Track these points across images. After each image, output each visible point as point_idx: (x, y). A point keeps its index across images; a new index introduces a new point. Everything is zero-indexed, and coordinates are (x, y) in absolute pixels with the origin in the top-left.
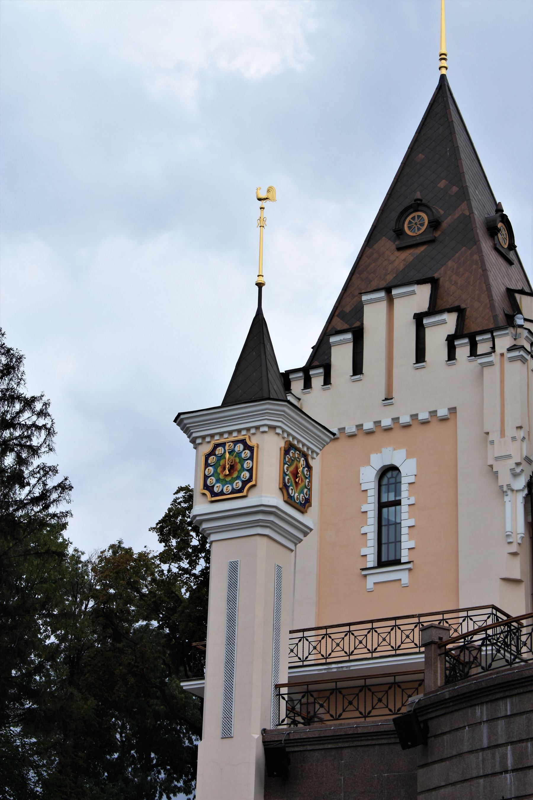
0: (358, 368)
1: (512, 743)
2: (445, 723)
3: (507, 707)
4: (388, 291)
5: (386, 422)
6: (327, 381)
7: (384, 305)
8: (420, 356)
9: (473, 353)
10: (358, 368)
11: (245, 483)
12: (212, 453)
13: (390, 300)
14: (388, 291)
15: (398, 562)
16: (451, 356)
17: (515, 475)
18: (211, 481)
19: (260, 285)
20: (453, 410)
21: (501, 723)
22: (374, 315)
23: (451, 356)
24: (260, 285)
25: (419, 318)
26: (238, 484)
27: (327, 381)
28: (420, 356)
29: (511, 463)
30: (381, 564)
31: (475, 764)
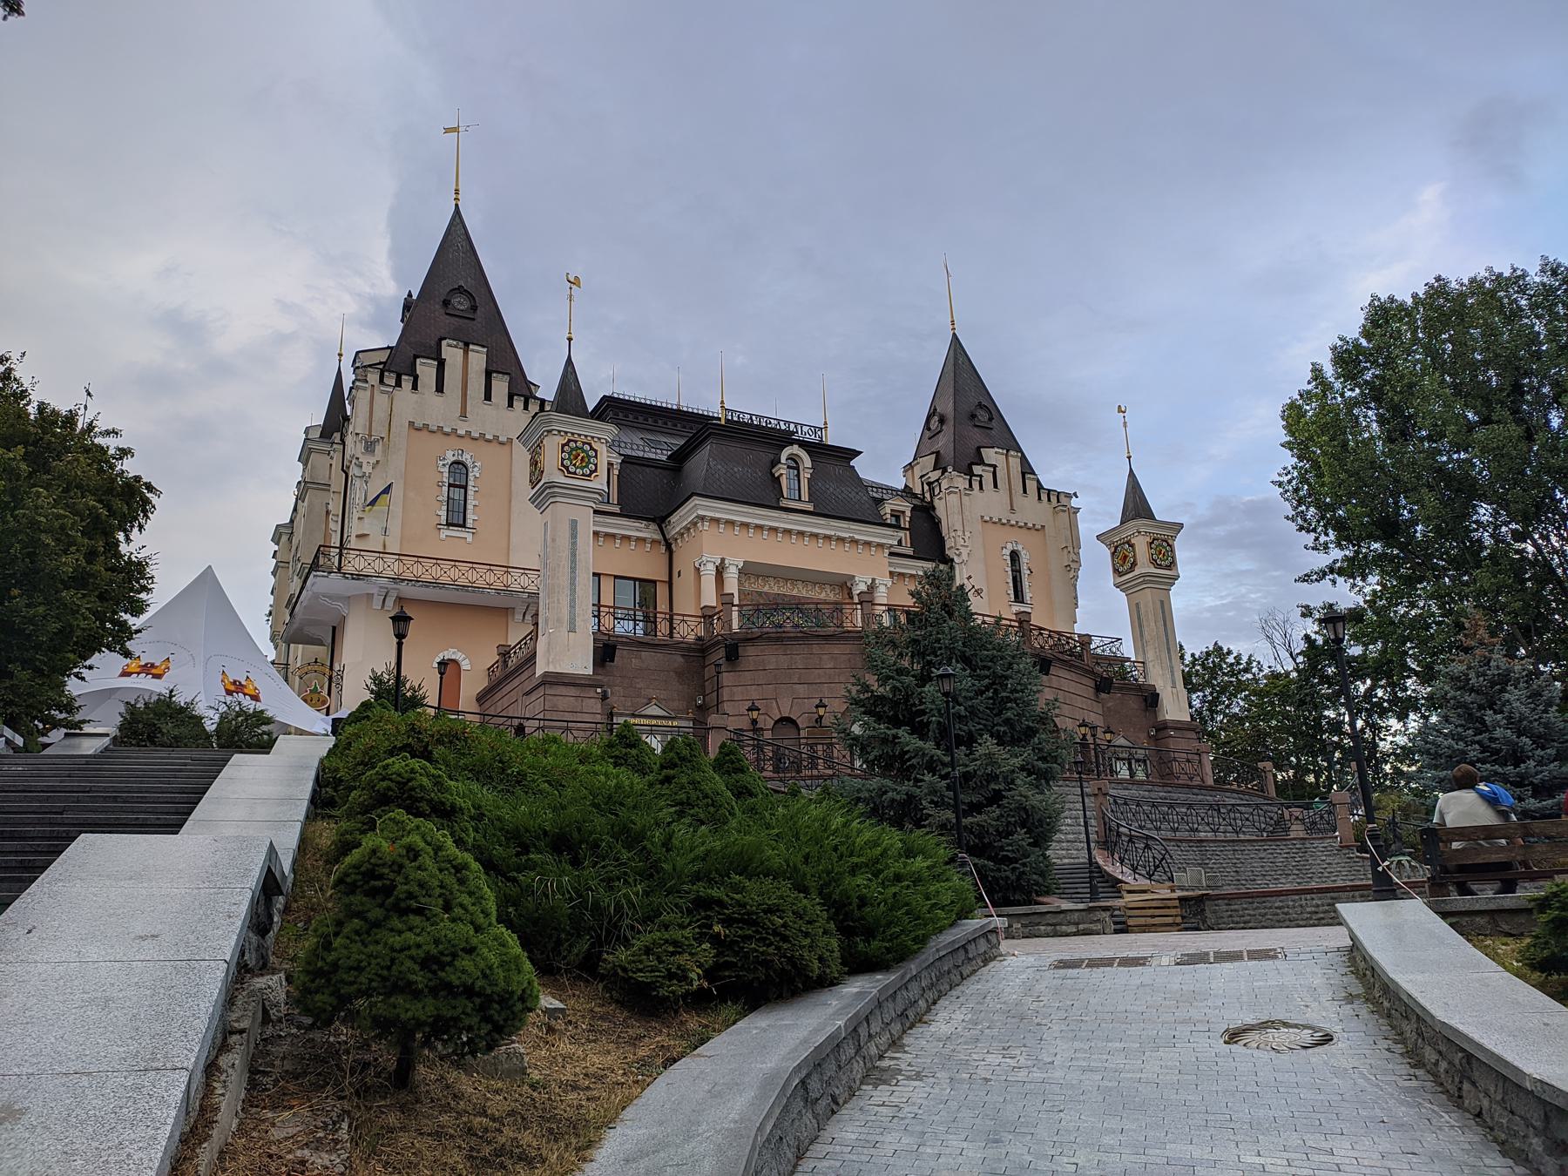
0: (440, 388)
4: (467, 344)
5: (461, 432)
6: (415, 387)
8: (488, 397)
9: (526, 408)
10: (440, 388)
11: (592, 472)
12: (567, 444)
13: (466, 352)
14: (467, 344)
15: (464, 526)
16: (511, 405)
18: (567, 462)
19: (570, 339)
23: (511, 405)
24: (570, 339)
27: (415, 387)
28: (488, 397)
30: (448, 524)
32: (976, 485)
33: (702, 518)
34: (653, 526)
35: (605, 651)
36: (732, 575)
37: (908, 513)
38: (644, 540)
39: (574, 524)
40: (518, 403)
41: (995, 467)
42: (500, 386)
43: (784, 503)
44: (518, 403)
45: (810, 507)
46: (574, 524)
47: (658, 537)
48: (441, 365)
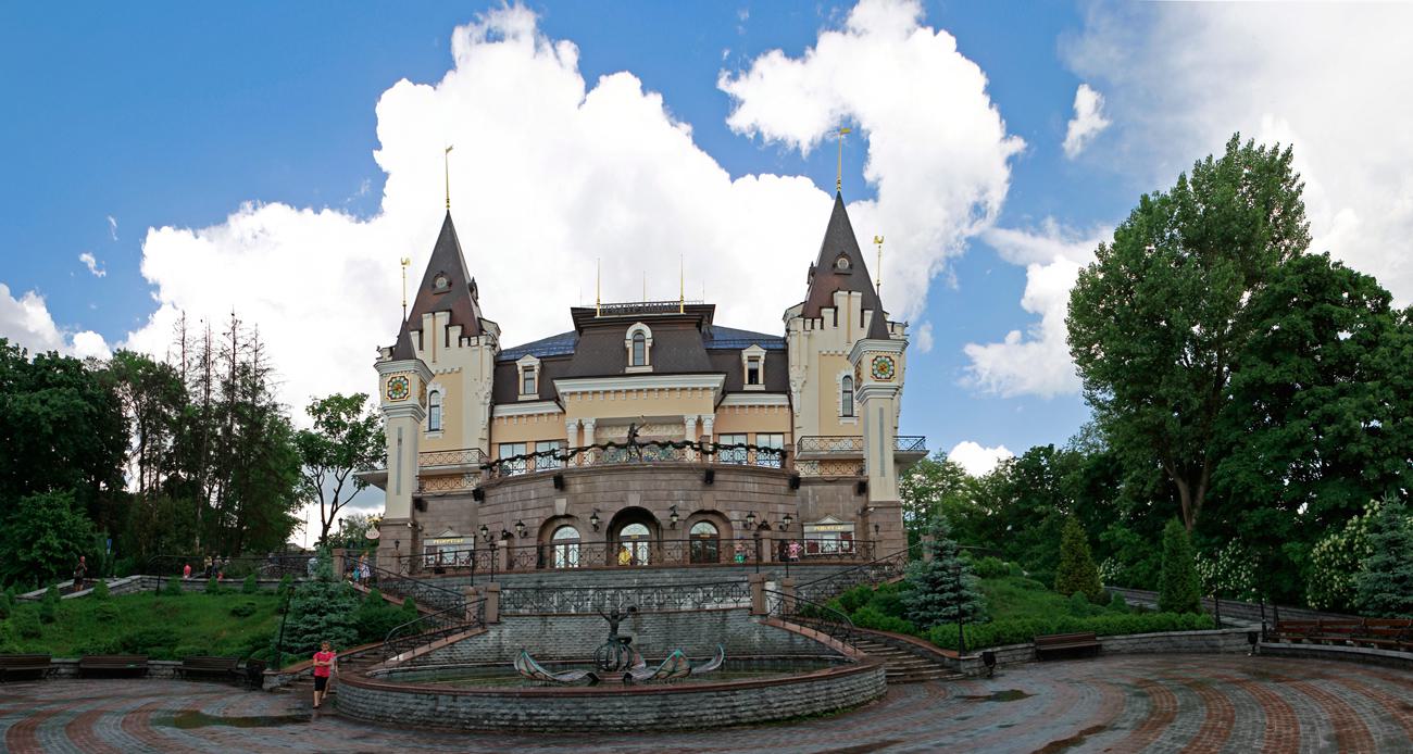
1: (508, 502)
2: (493, 492)
3: (518, 488)
7: (431, 319)
9: (469, 344)
13: (434, 317)
16: (460, 345)
17: (486, 398)
20: (460, 369)
21: (517, 494)
22: (427, 320)
23: (460, 345)
25: (447, 327)
26: (402, 395)
29: (484, 393)
31: (505, 507)
32: (818, 322)
33: (565, 394)
34: (553, 404)
35: (419, 504)
36: (589, 429)
37: (763, 357)
38: (553, 414)
39: (400, 429)
40: (465, 340)
41: (836, 309)
42: (455, 332)
43: (629, 370)
44: (465, 340)
45: (650, 369)
46: (400, 429)
47: (560, 410)
48: (421, 332)
